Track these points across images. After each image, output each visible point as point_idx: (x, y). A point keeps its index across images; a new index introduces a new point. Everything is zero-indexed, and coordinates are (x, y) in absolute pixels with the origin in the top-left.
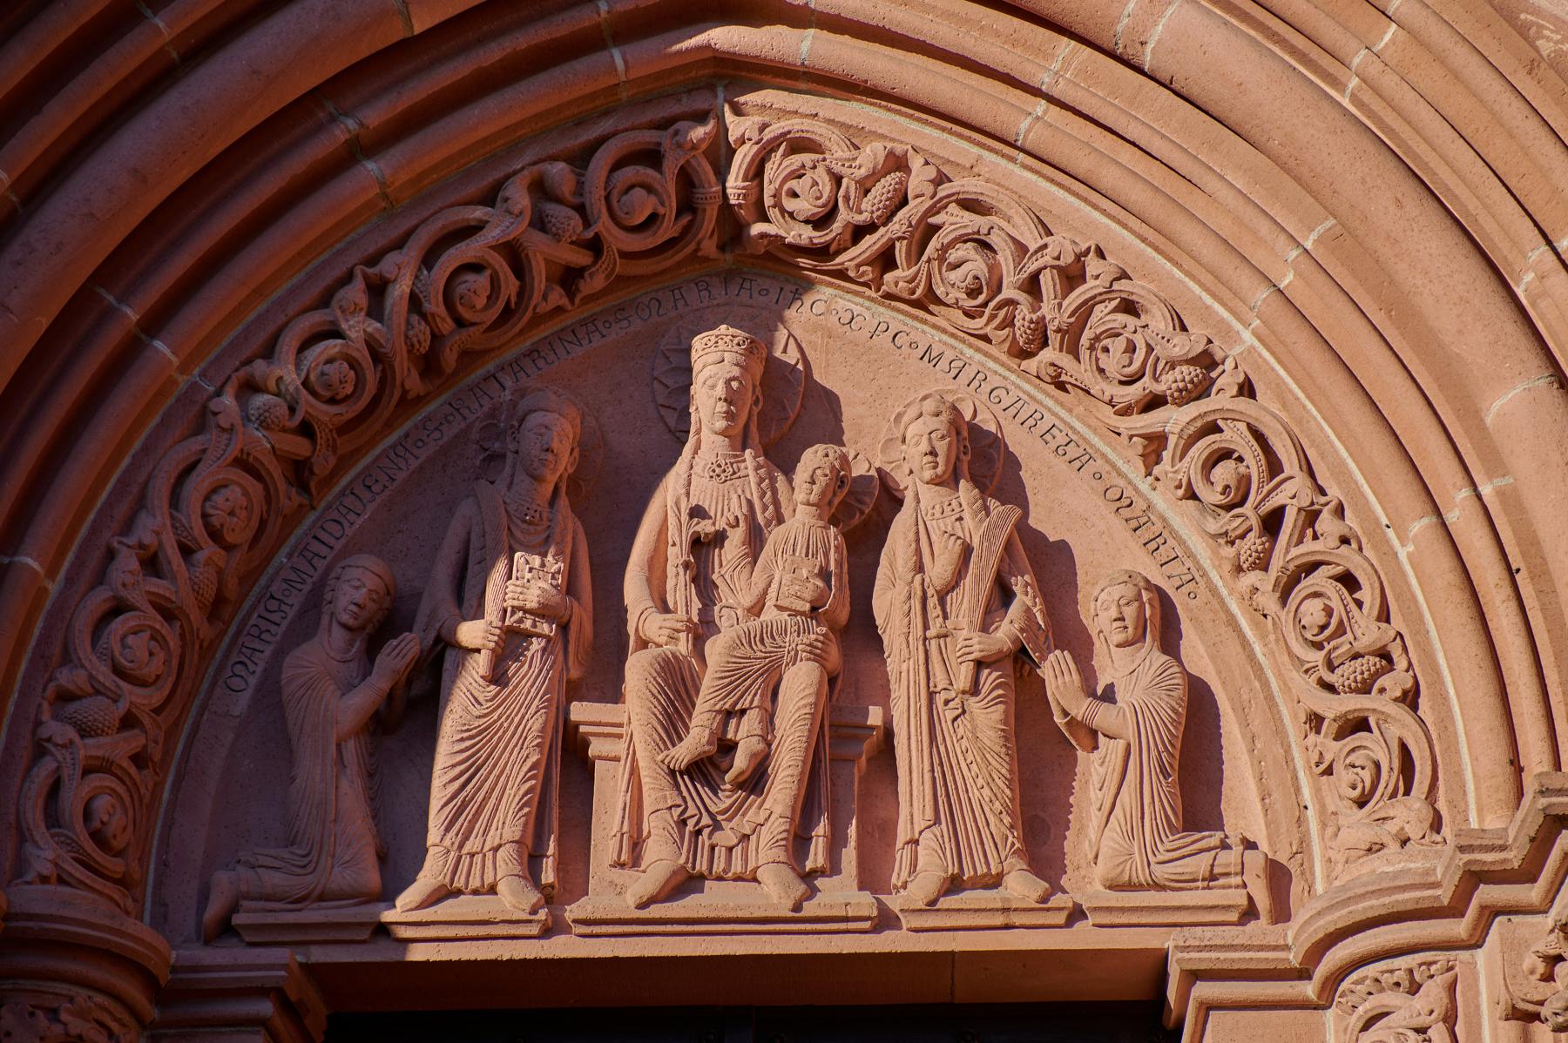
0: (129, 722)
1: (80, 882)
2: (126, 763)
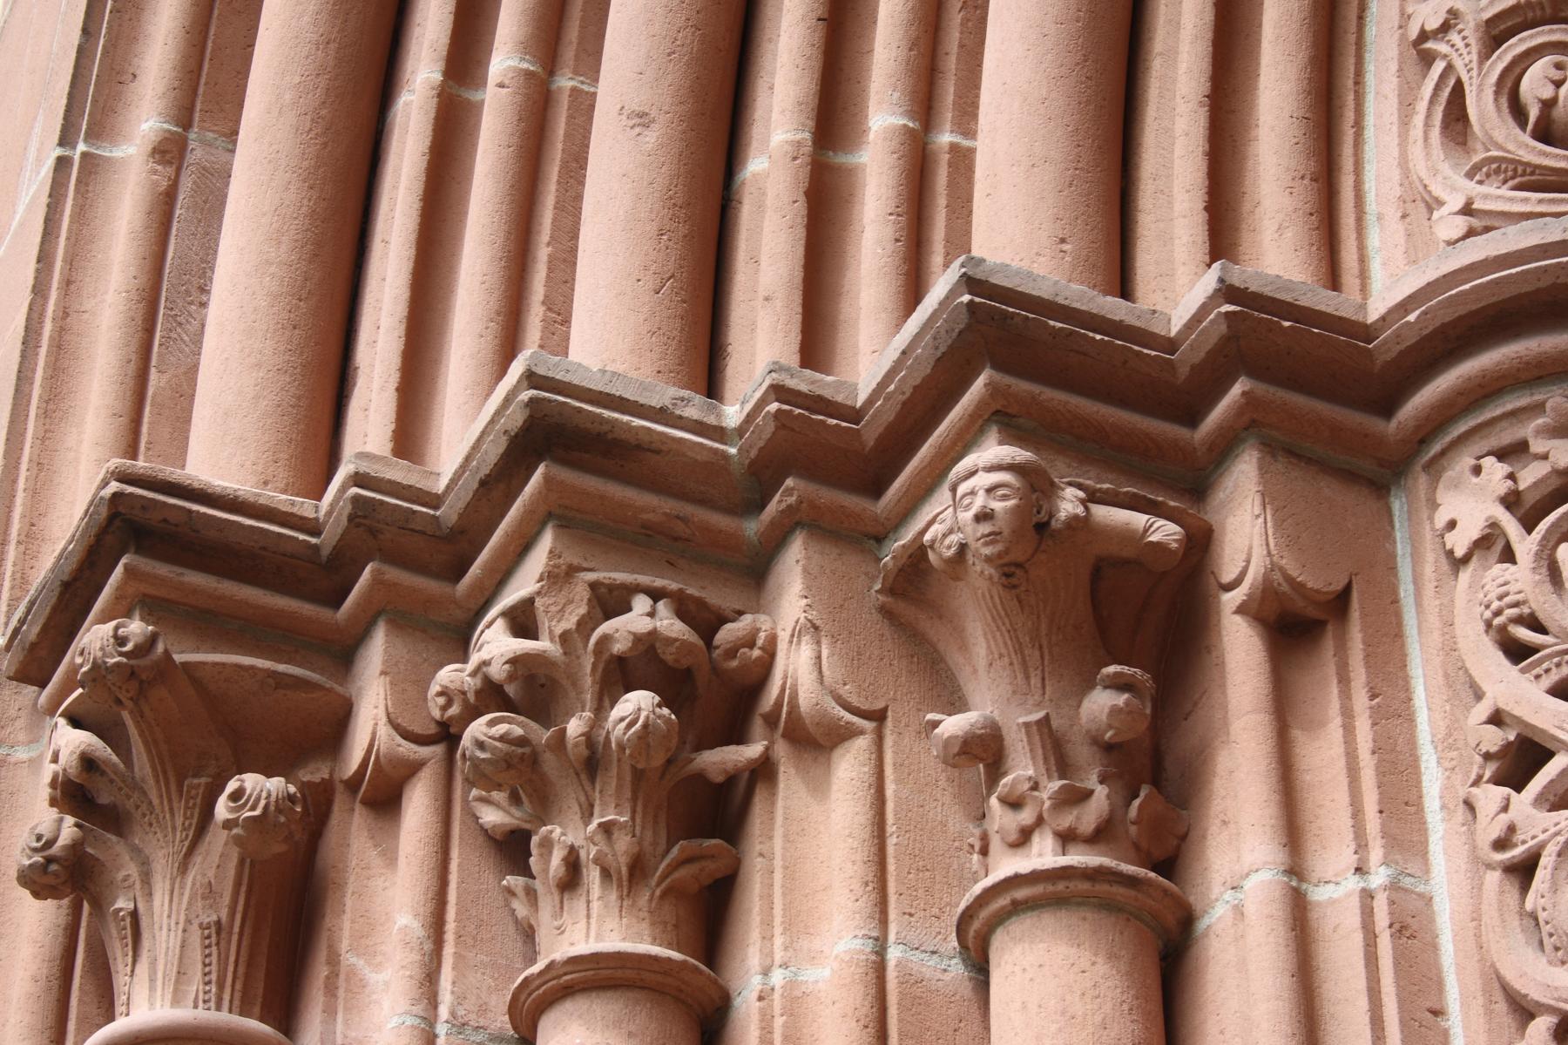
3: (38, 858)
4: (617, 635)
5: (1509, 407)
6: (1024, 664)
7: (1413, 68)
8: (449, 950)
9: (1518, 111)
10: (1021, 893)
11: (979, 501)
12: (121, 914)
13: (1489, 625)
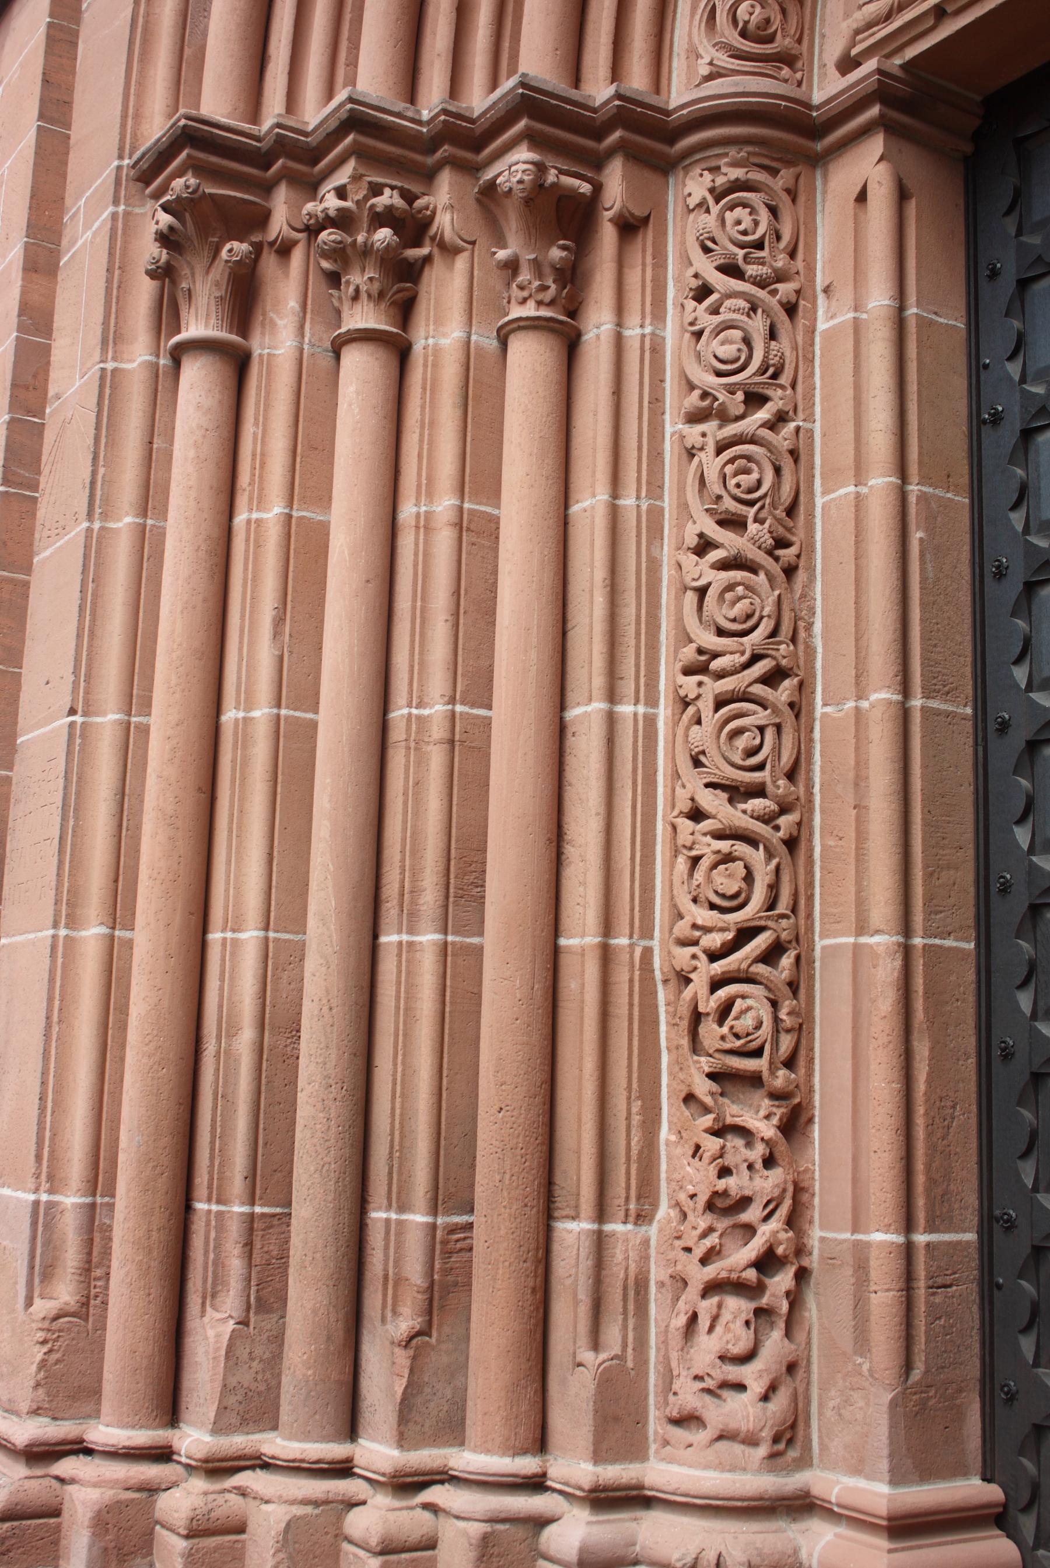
3: (153, 267)
6: (529, 234)
8: (308, 316)
10: (522, 324)
11: (519, 176)
13: (698, 238)
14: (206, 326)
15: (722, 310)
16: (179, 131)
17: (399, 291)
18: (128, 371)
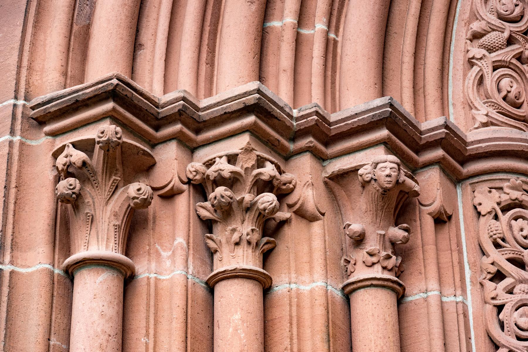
0: (510, 41)
1: (502, 122)
2: (514, 61)
3: (70, 192)
4: (265, 174)
5: (501, 177)
6: (377, 215)
7: (467, 65)
8: (191, 252)
9: (499, 91)
10: (375, 282)
11: (388, 172)
12: (89, 214)
14: (107, 247)
15: (515, 290)
16: (111, 88)
17: (266, 243)
18: (22, 274)
